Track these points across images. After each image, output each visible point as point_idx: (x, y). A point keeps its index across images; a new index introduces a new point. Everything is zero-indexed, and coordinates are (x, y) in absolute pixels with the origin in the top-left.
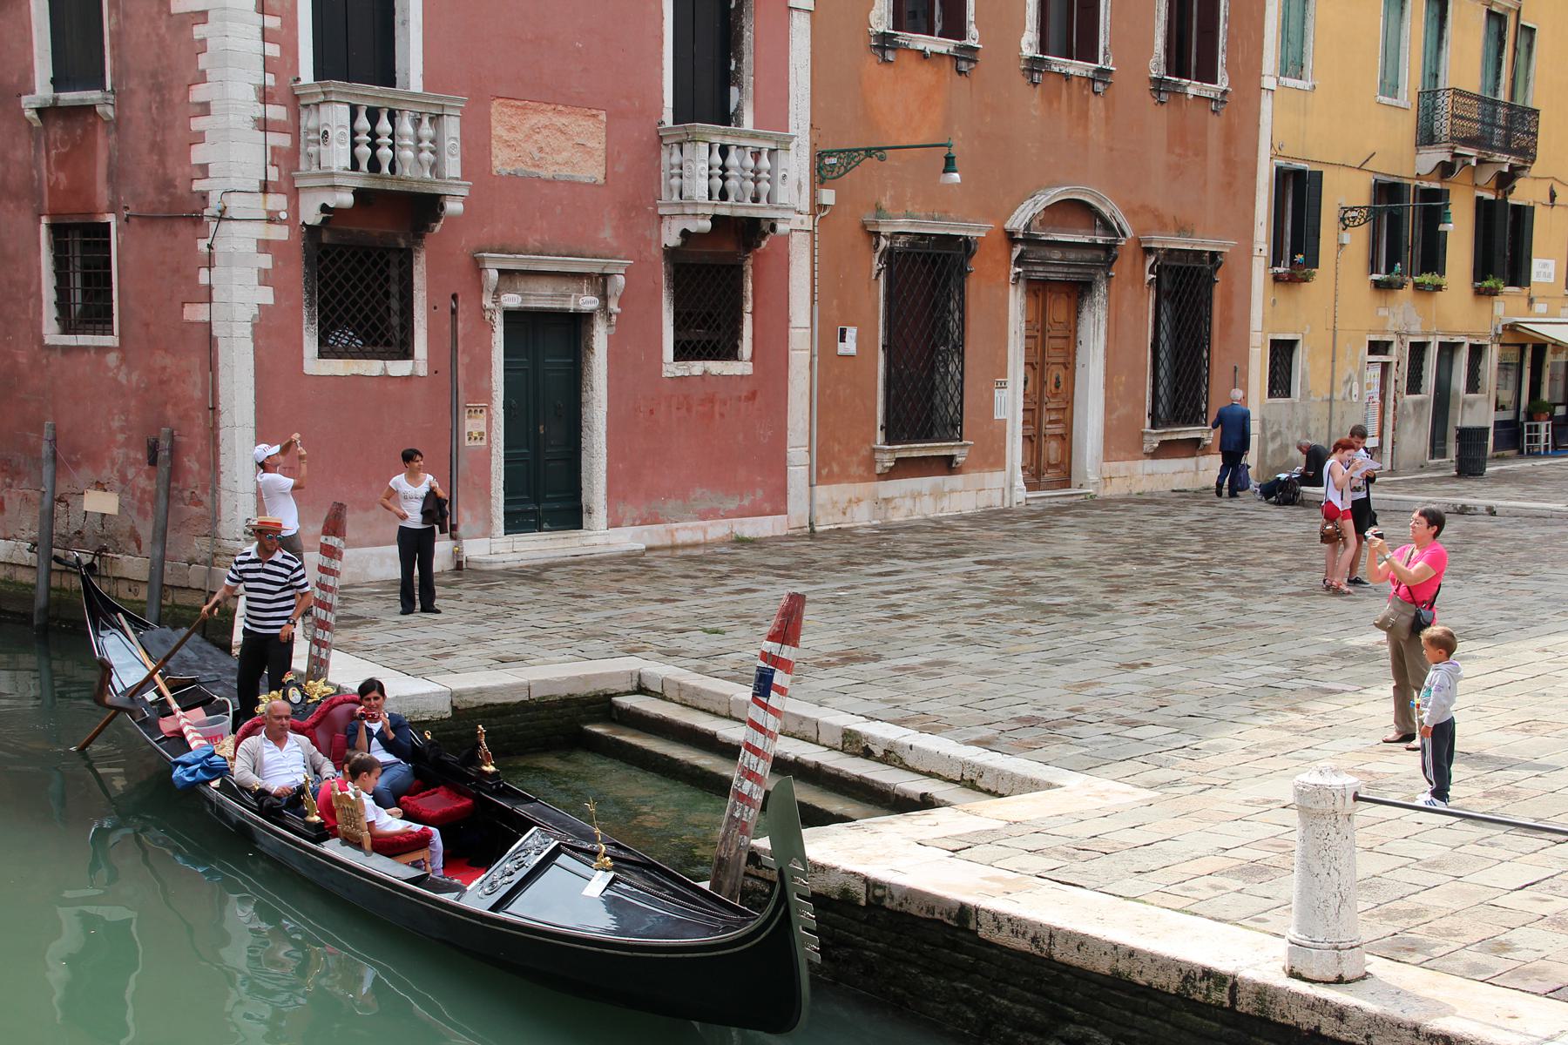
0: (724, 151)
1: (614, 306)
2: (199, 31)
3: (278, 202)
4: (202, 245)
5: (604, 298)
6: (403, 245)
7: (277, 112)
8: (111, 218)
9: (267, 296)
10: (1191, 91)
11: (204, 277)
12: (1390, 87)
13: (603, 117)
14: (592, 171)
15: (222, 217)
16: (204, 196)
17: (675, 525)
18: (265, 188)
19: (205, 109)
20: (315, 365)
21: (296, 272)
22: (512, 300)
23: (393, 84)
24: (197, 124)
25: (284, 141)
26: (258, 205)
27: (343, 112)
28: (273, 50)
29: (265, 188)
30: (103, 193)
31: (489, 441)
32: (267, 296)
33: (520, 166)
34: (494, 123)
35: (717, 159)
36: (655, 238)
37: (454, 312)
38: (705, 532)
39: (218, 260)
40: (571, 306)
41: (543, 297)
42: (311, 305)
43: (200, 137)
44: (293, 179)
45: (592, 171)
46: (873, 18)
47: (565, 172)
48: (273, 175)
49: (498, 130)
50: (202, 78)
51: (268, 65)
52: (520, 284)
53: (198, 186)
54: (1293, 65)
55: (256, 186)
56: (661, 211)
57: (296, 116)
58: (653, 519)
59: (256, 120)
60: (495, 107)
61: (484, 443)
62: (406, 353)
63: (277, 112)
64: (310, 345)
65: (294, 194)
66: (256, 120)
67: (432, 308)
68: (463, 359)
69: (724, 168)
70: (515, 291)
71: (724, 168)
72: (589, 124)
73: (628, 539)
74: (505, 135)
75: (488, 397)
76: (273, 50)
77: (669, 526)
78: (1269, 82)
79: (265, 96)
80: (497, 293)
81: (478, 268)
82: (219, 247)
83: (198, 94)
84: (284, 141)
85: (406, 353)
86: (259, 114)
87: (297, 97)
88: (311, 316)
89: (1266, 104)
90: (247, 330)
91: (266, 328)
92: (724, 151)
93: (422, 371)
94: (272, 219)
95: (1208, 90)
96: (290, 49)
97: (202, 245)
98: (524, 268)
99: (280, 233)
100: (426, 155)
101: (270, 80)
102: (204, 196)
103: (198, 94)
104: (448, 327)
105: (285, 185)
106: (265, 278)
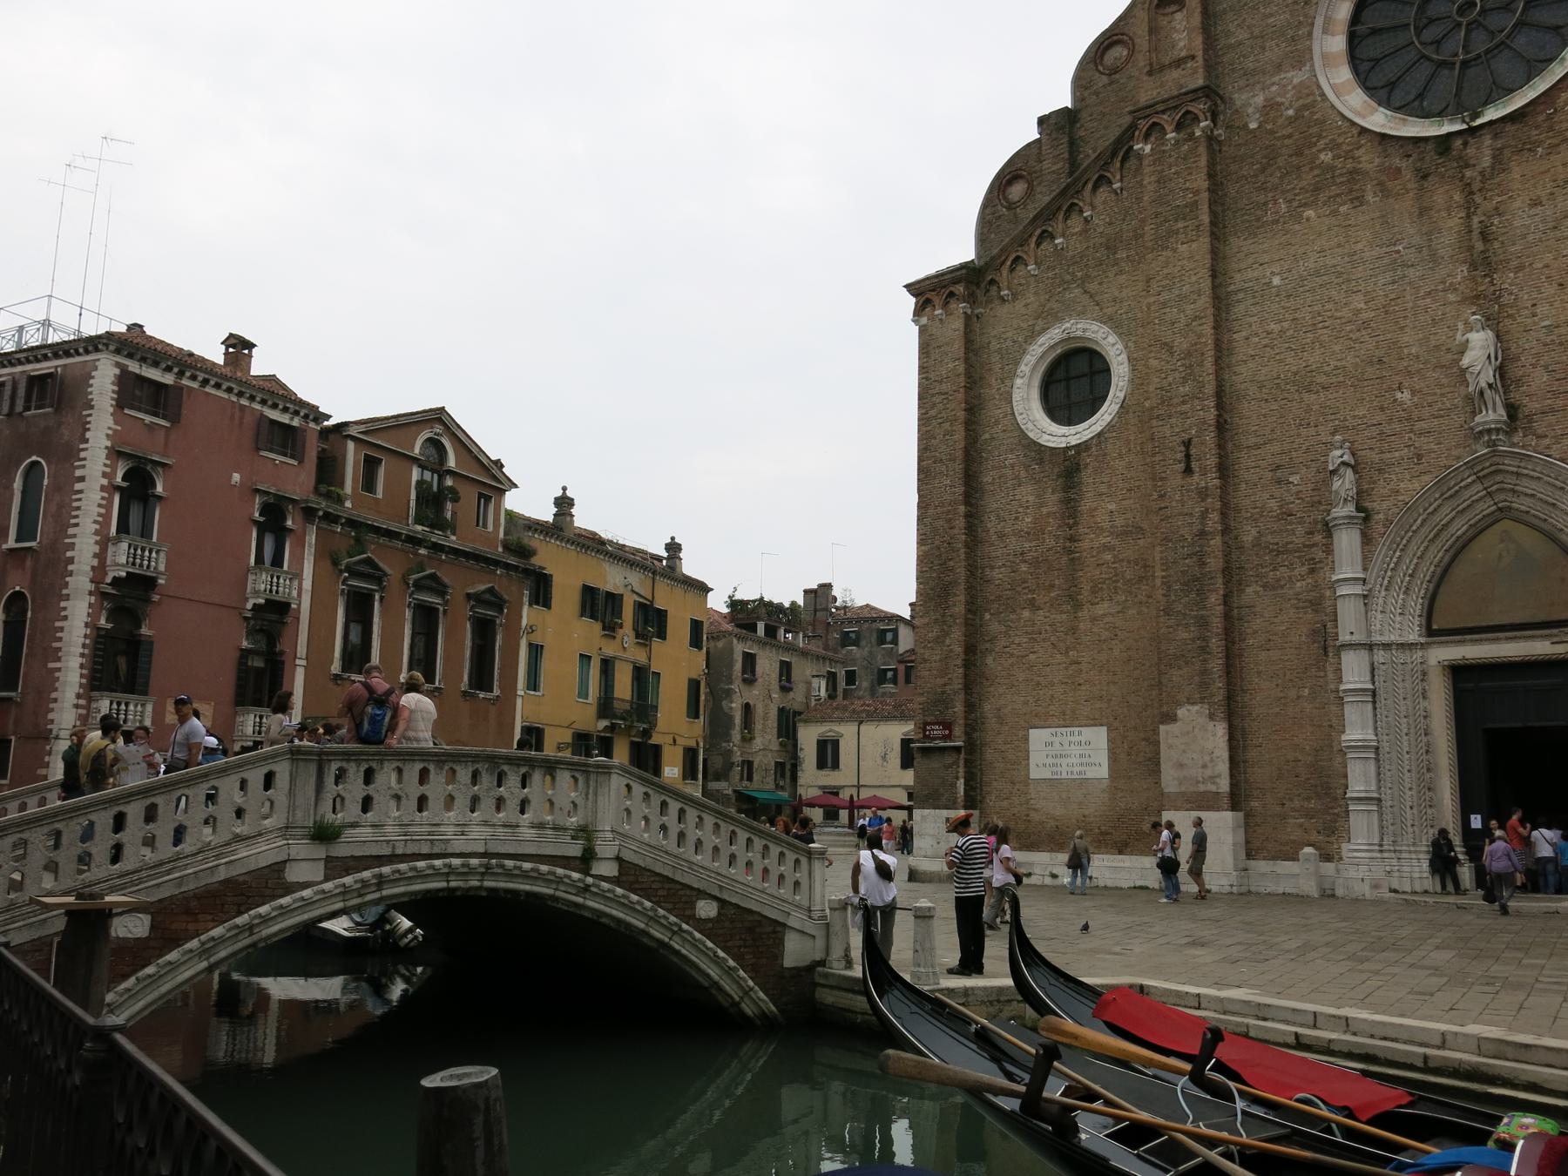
0: (261, 717)
2: (57, 674)
4: (48, 748)
7: (82, 702)
10: (481, 696)
11: (47, 759)
12: (583, 693)
15: (57, 738)
16: (51, 730)
19: (55, 700)
24: (51, 706)
25: (83, 712)
27: (108, 702)
30: (11, 727)
35: (258, 720)
39: (53, 752)
43: (52, 710)
46: (332, 668)
50: (56, 690)
53: (49, 727)
54: (533, 684)
63: (82, 702)
69: (260, 723)
71: (260, 723)
72: (207, 707)
78: (520, 693)
79: (78, 696)
82: (54, 748)
83: (54, 695)
89: (519, 702)
92: (261, 717)
95: (489, 695)
97: (48, 748)
100: (138, 717)
101: (81, 691)
102: (51, 730)
103: (54, 695)
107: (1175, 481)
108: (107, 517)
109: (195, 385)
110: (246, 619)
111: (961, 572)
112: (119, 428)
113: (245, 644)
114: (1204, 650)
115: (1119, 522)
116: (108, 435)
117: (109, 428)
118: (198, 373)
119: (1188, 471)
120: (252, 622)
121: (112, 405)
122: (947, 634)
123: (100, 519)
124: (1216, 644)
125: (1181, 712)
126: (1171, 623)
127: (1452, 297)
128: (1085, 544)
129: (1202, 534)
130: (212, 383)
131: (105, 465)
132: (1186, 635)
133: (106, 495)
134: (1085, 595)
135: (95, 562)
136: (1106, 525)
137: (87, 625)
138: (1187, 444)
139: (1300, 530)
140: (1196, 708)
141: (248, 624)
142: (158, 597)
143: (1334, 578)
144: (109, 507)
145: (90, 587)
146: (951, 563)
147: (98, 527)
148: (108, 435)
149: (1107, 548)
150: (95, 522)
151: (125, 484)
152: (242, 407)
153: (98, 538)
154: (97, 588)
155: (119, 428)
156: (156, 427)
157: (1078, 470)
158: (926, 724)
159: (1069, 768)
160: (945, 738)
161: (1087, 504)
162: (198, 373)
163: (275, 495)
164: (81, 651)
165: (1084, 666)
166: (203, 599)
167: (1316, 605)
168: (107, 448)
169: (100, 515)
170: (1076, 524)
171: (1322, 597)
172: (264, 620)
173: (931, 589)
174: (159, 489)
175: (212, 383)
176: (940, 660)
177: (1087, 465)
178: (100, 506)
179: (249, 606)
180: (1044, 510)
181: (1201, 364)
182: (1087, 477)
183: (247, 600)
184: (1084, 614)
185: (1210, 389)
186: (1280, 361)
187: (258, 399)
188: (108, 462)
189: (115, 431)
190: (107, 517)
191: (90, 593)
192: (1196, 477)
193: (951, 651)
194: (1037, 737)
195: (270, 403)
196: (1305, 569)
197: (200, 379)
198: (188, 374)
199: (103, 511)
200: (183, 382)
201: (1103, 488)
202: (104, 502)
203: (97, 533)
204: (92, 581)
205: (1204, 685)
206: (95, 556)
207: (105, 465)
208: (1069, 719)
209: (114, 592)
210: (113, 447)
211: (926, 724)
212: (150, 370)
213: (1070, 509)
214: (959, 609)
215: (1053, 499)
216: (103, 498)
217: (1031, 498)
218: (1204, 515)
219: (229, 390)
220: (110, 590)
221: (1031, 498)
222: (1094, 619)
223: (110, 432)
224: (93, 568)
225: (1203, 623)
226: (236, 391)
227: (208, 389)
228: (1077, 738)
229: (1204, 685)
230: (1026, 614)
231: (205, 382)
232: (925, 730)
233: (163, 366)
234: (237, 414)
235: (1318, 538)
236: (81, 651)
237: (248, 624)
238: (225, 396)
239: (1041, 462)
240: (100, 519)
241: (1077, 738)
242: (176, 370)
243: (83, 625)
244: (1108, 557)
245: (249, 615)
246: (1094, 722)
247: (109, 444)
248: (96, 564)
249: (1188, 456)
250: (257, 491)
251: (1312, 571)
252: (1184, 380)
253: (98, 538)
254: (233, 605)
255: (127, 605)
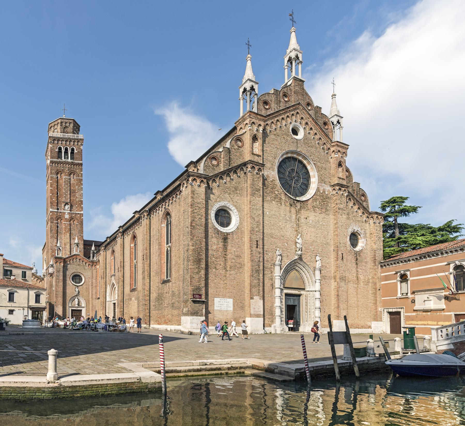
107: (254, 248)
111: (204, 256)
114: (259, 285)
115: (236, 253)
119: (257, 247)
122: (200, 272)
124: (261, 284)
125: (255, 297)
126: (253, 278)
127: (293, 229)
128: (229, 257)
129: (259, 261)
132: (256, 282)
134: (228, 269)
136: (233, 253)
138: (257, 241)
139: (270, 265)
140: (258, 297)
143: (275, 275)
146: (201, 253)
149: (233, 259)
157: (227, 239)
158: (194, 294)
159: (224, 308)
160: (199, 298)
161: (229, 248)
165: (228, 285)
167: (272, 279)
170: (226, 251)
171: (273, 278)
173: (195, 259)
176: (198, 278)
177: (229, 238)
180: (219, 246)
181: (260, 225)
182: (229, 241)
184: (228, 272)
185: (261, 231)
186: (268, 230)
192: (258, 249)
193: (201, 276)
194: (216, 300)
196: (270, 272)
201: (233, 245)
205: (259, 292)
208: (224, 296)
211: (194, 294)
213: (225, 247)
214: (203, 266)
215: (221, 244)
217: (216, 242)
218: (260, 257)
221: (216, 242)
222: (230, 275)
225: (259, 280)
228: (226, 301)
229: (259, 292)
230: (214, 270)
232: (194, 296)
235: (272, 267)
239: (218, 234)
241: (226, 301)
244: (233, 261)
246: (230, 297)
249: (257, 244)
251: (271, 273)
252: (257, 228)
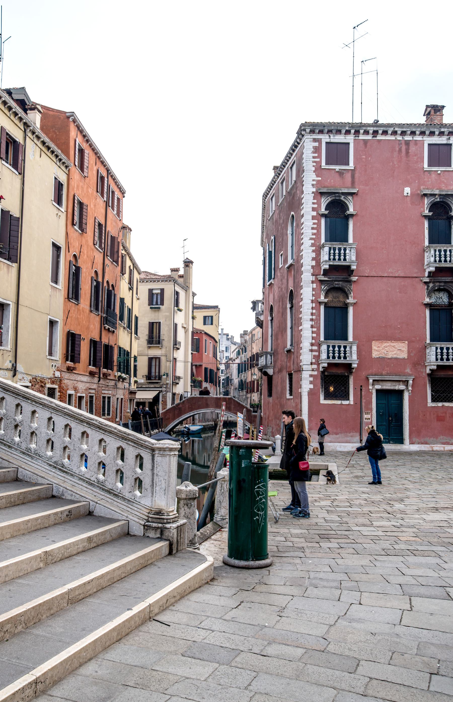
1: (410, 388)
3: (315, 366)
5: (407, 386)
6: (346, 374)
8: (293, 372)
9: (312, 386)
13: (407, 342)
14: (404, 355)
17: (433, 445)
18: (312, 364)
20: (322, 401)
21: (319, 381)
22: (378, 387)
23: (347, 340)
25: (317, 354)
26: (310, 367)
28: (314, 335)
29: (312, 364)
31: (372, 420)
32: (312, 386)
33: (381, 355)
34: (373, 346)
36: (424, 370)
37: (361, 390)
38: (444, 448)
40: (397, 388)
41: (388, 386)
42: (322, 388)
44: (318, 362)
45: (404, 355)
47: (395, 356)
48: (314, 361)
49: (374, 347)
51: (313, 338)
52: (381, 383)
55: (309, 363)
56: (426, 364)
57: (319, 348)
58: (426, 443)
59: (310, 350)
60: (373, 343)
61: (370, 421)
62: (348, 399)
63: (315, 348)
64: (322, 397)
65: (318, 365)
66: (310, 350)
67: (355, 389)
68: (364, 401)
70: (379, 385)
73: (415, 448)
74: (376, 349)
75: (371, 410)
76: (314, 335)
77: (431, 445)
79: (312, 345)
80: (373, 385)
81: (367, 379)
84: (317, 354)
85: (348, 399)
86: (311, 348)
87: (320, 344)
88: (322, 391)
90: (307, 394)
91: (311, 393)
93: (352, 403)
94: (313, 370)
96: (318, 334)
98: (381, 379)
99: (316, 373)
104: (359, 393)
105: (316, 363)
106: (311, 383)
108: (318, 234)
109: (369, 137)
110: (425, 283)
112: (320, 179)
113: (427, 300)
116: (313, 185)
117: (313, 180)
118: (368, 128)
120: (431, 285)
121: (314, 166)
123: (314, 237)
130: (380, 132)
131: (314, 203)
133: (316, 221)
135: (314, 263)
137: (312, 301)
141: (428, 286)
142: (357, 278)
144: (318, 228)
145: (313, 278)
147: (313, 241)
148: (313, 185)
150: (311, 239)
151: (327, 212)
152: (407, 143)
153: (314, 248)
154: (316, 278)
155: (320, 179)
156: (344, 172)
162: (368, 128)
163: (440, 195)
164: (311, 317)
166: (391, 275)
168: (313, 193)
169: (313, 234)
172: (440, 282)
174: (351, 210)
175: (380, 132)
178: (313, 228)
179: (426, 274)
183: (425, 270)
187: (418, 133)
188: (315, 201)
189: (318, 181)
190: (318, 234)
191: (313, 282)
195: (427, 133)
197: (371, 132)
198: (362, 131)
199: (315, 231)
200: (360, 138)
202: (315, 226)
203: (313, 245)
204: (313, 275)
206: (313, 259)
207: (314, 203)
209: (326, 279)
210: (317, 191)
212: (336, 137)
216: (314, 224)
219: (394, 133)
220: (323, 278)
223: (315, 183)
224: (313, 267)
226: (399, 132)
227: (379, 137)
231: (375, 133)
233: (343, 131)
234: (404, 148)
236: (311, 317)
237: (428, 286)
238: (393, 138)
240: (314, 237)
242: (353, 131)
243: (310, 301)
245: (427, 280)
247: (314, 190)
248: (314, 265)
250: (425, 195)
253: (314, 248)
254: (415, 275)
255: (336, 286)
